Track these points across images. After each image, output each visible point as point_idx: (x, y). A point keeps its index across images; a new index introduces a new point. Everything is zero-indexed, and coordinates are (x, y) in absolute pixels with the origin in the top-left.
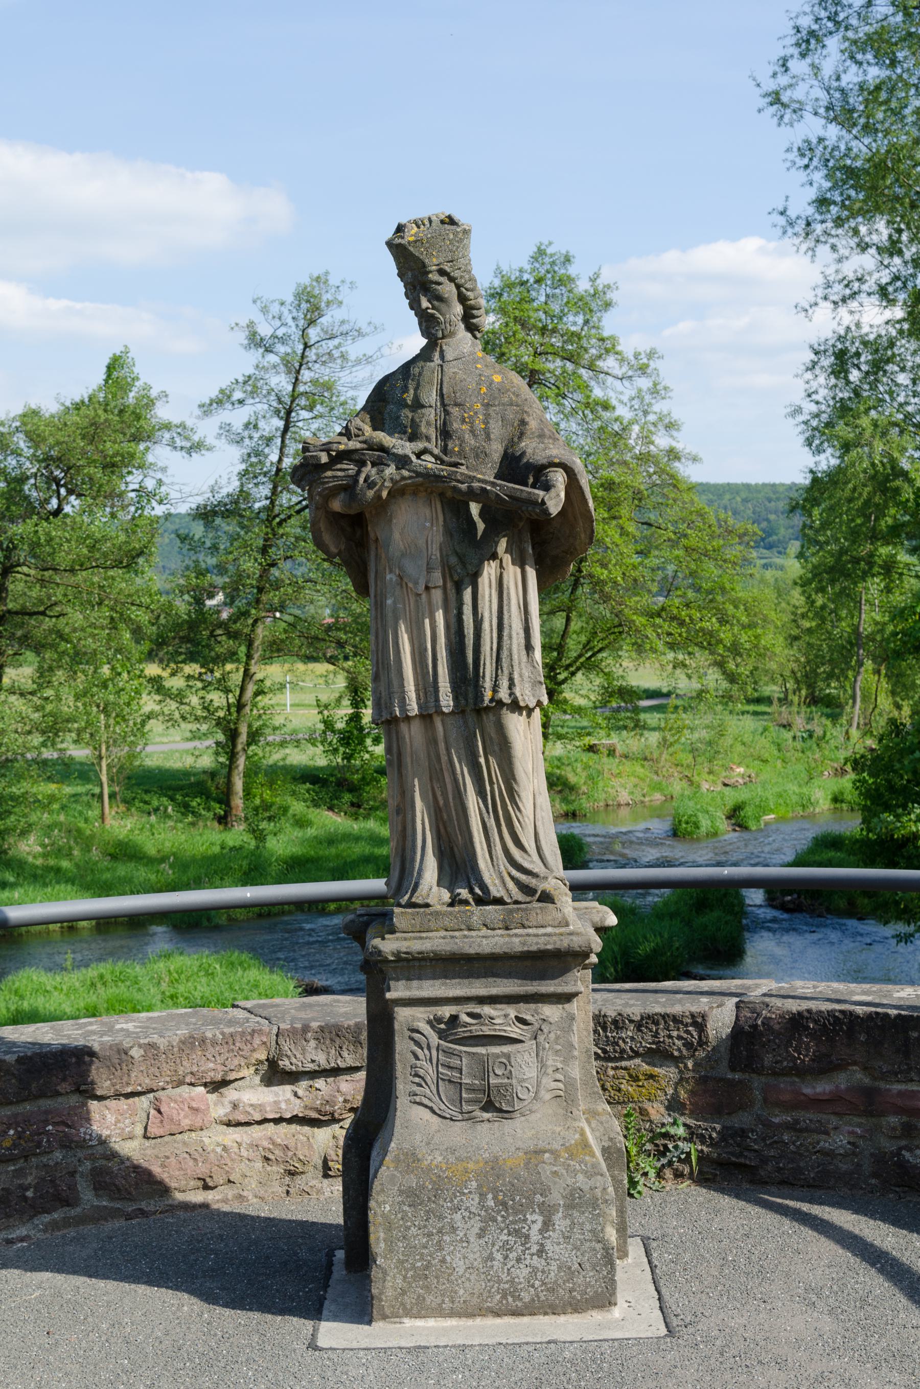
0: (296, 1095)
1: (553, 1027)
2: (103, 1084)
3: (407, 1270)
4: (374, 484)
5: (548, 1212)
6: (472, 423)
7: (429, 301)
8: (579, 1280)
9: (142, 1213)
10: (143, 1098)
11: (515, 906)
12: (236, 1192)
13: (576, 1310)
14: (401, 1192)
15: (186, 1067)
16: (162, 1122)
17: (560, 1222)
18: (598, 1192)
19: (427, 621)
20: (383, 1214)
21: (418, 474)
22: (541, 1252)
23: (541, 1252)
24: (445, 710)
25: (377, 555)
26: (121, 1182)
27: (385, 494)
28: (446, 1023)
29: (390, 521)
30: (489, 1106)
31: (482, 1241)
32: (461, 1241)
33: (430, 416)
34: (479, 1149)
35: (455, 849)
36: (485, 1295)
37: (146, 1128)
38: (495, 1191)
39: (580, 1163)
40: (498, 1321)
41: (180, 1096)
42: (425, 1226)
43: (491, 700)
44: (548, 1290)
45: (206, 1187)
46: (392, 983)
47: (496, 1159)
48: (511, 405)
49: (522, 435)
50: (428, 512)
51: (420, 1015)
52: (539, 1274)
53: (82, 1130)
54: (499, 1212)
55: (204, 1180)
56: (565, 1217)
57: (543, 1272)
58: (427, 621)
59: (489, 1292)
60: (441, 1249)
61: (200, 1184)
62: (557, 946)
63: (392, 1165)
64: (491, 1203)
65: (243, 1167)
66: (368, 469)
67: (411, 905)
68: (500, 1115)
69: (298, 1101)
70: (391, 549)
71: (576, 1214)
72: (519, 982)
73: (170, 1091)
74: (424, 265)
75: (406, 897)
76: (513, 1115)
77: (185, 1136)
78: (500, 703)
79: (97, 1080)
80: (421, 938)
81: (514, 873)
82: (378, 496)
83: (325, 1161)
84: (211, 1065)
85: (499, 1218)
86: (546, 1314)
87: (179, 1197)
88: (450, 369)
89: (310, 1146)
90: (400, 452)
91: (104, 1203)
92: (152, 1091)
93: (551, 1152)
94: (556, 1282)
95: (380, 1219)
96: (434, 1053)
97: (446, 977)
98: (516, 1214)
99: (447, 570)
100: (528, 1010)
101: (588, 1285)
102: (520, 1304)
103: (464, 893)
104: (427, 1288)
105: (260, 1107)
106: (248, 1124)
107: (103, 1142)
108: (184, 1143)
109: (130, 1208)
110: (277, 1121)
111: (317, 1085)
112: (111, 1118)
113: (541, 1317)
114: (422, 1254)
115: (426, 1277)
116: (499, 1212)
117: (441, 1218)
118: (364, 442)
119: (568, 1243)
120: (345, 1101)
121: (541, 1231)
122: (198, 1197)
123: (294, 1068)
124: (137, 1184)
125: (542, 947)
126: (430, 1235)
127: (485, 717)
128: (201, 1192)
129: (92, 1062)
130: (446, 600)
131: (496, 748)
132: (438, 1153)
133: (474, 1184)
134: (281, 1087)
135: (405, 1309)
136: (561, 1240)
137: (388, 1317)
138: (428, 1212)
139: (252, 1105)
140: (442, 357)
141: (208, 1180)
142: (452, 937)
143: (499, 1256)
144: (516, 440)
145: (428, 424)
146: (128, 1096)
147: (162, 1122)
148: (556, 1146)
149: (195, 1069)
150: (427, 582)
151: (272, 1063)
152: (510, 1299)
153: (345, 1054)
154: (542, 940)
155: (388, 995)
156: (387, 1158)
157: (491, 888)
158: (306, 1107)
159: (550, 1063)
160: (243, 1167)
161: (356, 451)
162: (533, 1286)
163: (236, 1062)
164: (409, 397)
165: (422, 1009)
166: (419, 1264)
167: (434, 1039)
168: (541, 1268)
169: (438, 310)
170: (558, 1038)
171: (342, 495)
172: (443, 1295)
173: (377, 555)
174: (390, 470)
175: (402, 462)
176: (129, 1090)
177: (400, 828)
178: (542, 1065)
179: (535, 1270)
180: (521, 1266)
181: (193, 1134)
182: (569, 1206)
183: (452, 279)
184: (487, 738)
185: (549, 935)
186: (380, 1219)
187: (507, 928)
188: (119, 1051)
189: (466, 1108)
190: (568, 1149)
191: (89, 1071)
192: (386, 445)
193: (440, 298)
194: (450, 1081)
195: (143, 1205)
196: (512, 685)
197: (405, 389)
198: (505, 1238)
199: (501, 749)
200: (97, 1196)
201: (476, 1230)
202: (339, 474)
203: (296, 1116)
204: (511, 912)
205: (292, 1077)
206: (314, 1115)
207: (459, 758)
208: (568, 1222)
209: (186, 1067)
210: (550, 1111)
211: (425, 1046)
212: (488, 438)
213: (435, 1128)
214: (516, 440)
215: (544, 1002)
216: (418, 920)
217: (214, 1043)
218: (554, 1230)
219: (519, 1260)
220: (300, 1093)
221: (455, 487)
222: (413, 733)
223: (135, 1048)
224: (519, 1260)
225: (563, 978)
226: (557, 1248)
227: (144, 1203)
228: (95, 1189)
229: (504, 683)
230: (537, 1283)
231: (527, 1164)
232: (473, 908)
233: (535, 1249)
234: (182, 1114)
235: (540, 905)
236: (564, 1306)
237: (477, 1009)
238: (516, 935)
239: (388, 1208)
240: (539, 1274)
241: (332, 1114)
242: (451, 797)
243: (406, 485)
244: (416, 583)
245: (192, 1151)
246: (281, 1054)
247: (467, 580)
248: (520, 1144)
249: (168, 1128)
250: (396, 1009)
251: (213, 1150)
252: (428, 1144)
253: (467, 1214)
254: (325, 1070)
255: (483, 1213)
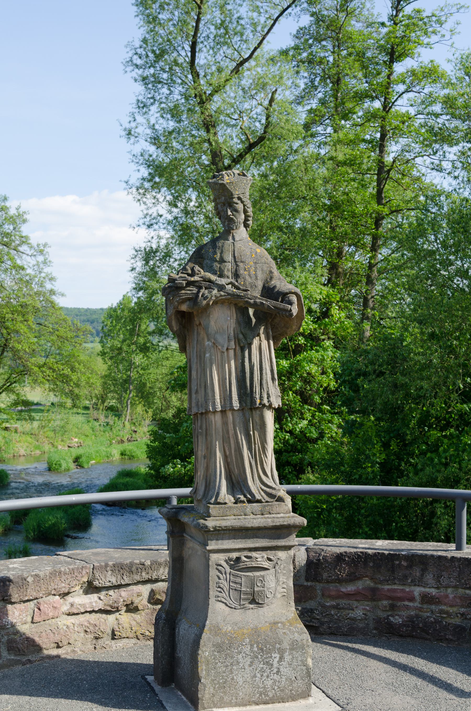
0: (100, 598)
1: (283, 562)
2: (15, 595)
3: (215, 684)
4: (207, 297)
5: (281, 652)
6: (249, 271)
7: (231, 212)
8: (295, 685)
9: (30, 661)
10: (31, 603)
11: (267, 504)
12: (72, 649)
13: (293, 700)
14: (214, 645)
15: (53, 586)
16: (40, 614)
17: (287, 657)
18: (305, 642)
19: (227, 365)
20: (205, 657)
21: (229, 294)
22: (278, 672)
23: (278, 672)
24: (235, 408)
25: (198, 332)
26: (20, 646)
27: (211, 303)
28: (233, 561)
29: (209, 316)
30: (253, 601)
31: (251, 668)
32: (242, 668)
33: (229, 267)
34: (248, 623)
35: (233, 476)
36: (252, 694)
37: (33, 618)
38: (258, 643)
39: (295, 628)
40: (257, 707)
41: (49, 601)
42: (225, 662)
43: (260, 404)
44: (281, 691)
45: (58, 647)
46: (209, 542)
47: (256, 628)
48: (265, 263)
49: (271, 278)
50: (229, 313)
51: (221, 557)
52: (277, 683)
53: (4, 620)
54: (259, 653)
55: (58, 643)
56: (289, 655)
57: (279, 682)
58: (227, 365)
59: (254, 693)
60: (232, 673)
61: (56, 645)
62: (289, 523)
63: (208, 632)
64: (256, 649)
65: (75, 636)
66: (203, 291)
67: (217, 503)
68: (258, 605)
69: (101, 602)
70: (210, 330)
71: (294, 653)
72: (268, 540)
73: (44, 599)
74: (232, 194)
75: (213, 499)
76: (263, 605)
77: (50, 621)
78: (264, 405)
79: (12, 594)
80: (224, 520)
81: (263, 487)
82: (208, 304)
83: (113, 631)
84: (63, 585)
85: (259, 656)
86: (279, 702)
87: (46, 652)
88: (238, 245)
89: (106, 624)
90: (220, 283)
91: (12, 657)
92: (37, 599)
93: (282, 623)
94: (284, 686)
95: (203, 660)
96: (228, 576)
97: (235, 539)
98: (267, 654)
99: (237, 340)
100: (271, 554)
101: (299, 687)
102: (267, 698)
103: (242, 498)
104: (225, 693)
105: (83, 605)
106: (78, 614)
107: (13, 626)
108: (50, 625)
109: (24, 659)
110: (90, 612)
111: (110, 594)
112: (17, 613)
113: (277, 704)
114: (223, 676)
115: (224, 687)
116: (259, 653)
117: (232, 657)
118: (202, 277)
119: (291, 667)
120: (124, 601)
121: (278, 662)
122: (54, 652)
123: (100, 585)
124: (28, 647)
125: (282, 523)
126: (227, 666)
127: (254, 412)
128: (55, 649)
129: (10, 585)
130: (235, 355)
131: (259, 427)
132: (229, 625)
133: (248, 640)
134: (92, 595)
135: (214, 704)
136: (287, 666)
137: (206, 708)
138: (226, 655)
139: (80, 604)
140: (234, 239)
141: (60, 643)
142: (239, 519)
143: (259, 675)
144: (268, 280)
145: (228, 270)
146: (25, 602)
147: (40, 614)
148: (283, 620)
149: (56, 587)
150: (228, 346)
151: (90, 583)
152: (263, 696)
153: (125, 577)
154: (281, 520)
155: (208, 548)
156: (205, 629)
157: (256, 495)
158: (105, 605)
159: (281, 579)
160: (75, 636)
161: (197, 281)
162: (274, 689)
163: (74, 583)
164: (218, 257)
165: (222, 554)
166: (221, 681)
167: (228, 569)
168: (278, 680)
169: (235, 216)
170: (284, 567)
171: (188, 303)
172: (232, 696)
173: (198, 332)
174: (215, 292)
175: (221, 288)
176: (26, 598)
177: (205, 466)
178: (278, 581)
179: (275, 681)
180: (269, 679)
181: (53, 620)
182: (291, 649)
183: (242, 202)
184: (254, 422)
185: (283, 517)
186: (203, 660)
187: (262, 514)
188: (22, 579)
189: (242, 602)
190: (289, 621)
191: (8, 589)
192: (212, 279)
193: (236, 211)
194: (235, 590)
195: (30, 657)
196: (269, 397)
197: (215, 253)
198: (262, 666)
199: (261, 428)
200: (9, 654)
201: (249, 663)
202: (188, 292)
203: (100, 609)
204: (265, 506)
205: (97, 590)
206: (109, 608)
207: (240, 432)
208: (291, 657)
209: (53, 586)
210: (280, 603)
211: (223, 573)
212: (256, 279)
213: (227, 613)
214: (268, 280)
215: (278, 550)
216: (221, 511)
217: (65, 574)
218: (284, 661)
219: (268, 677)
220: (102, 597)
221: (247, 301)
222: (216, 419)
223: (30, 577)
224: (268, 677)
225: (288, 538)
226: (285, 670)
227: (30, 656)
228: (8, 650)
229: (265, 396)
230: (276, 688)
231: (271, 629)
232: (246, 504)
233: (275, 670)
234: (50, 610)
235: (278, 503)
236: (288, 698)
237: (249, 554)
238: (268, 518)
239: (207, 654)
240: (277, 683)
241: (117, 608)
242: (233, 452)
243: (222, 299)
244: (223, 347)
245: (52, 629)
246: (94, 578)
247: (246, 346)
248: (267, 620)
249: (43, 617)
250: (210, 555)
251: (62, 628)
252: (224, 621)
253: (244, 655)
254: (115, 586)
255: (252, 654)
